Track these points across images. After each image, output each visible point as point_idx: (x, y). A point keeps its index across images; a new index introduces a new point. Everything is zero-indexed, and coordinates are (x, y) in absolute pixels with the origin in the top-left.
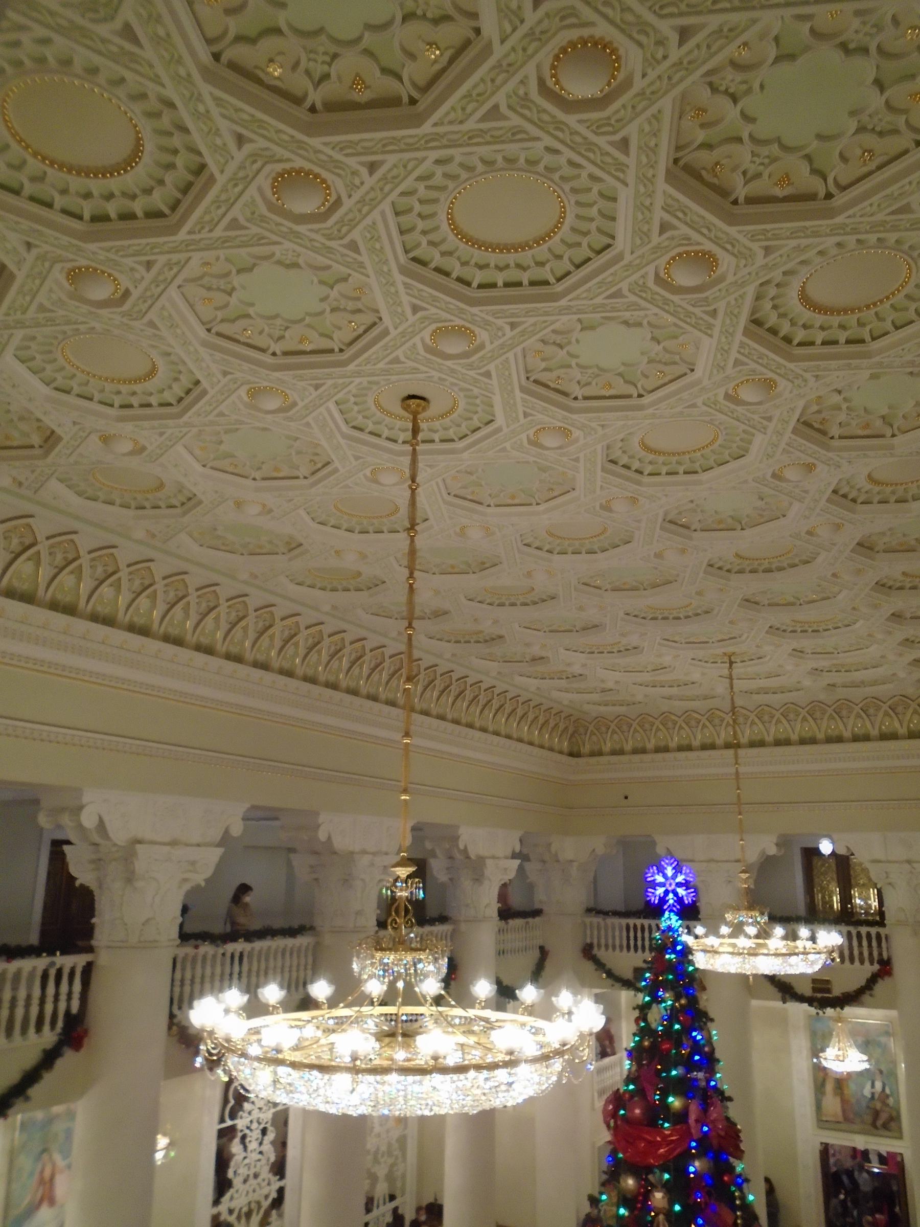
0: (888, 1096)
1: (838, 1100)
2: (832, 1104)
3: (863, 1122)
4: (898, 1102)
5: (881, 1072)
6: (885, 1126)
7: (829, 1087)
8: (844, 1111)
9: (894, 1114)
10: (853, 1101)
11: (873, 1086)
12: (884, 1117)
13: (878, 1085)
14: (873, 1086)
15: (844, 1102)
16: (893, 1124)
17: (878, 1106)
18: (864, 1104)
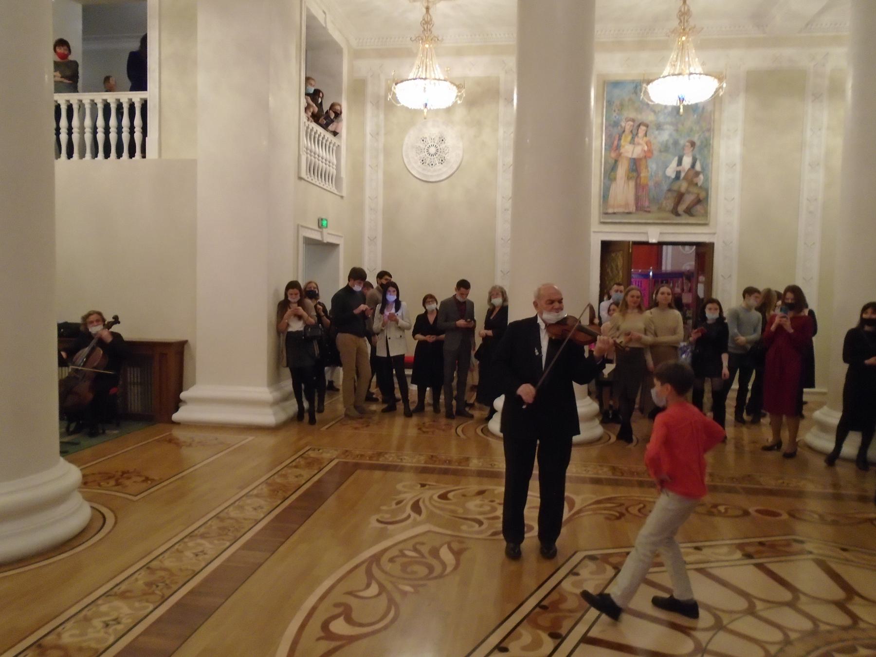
0: (697, 174)
1: (632, 184)
2: (623, 192)
3: (660, 209)
4: (707, 179)
5: (693, 144)
6: (689, 212)
7: (622, 171)
8: (637, 199)
9: (702, 195)
10: (651, 184)
11: (680, 163)
12: (689, 199)
13: (687, 161)
14: (680, 163)
15: (638, 186)
16: (699, 207)
17: (684, 186)
18: (665, 187)
